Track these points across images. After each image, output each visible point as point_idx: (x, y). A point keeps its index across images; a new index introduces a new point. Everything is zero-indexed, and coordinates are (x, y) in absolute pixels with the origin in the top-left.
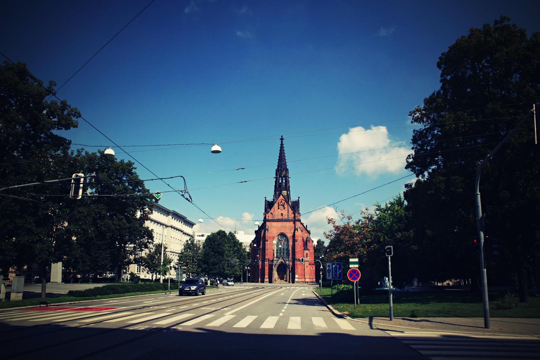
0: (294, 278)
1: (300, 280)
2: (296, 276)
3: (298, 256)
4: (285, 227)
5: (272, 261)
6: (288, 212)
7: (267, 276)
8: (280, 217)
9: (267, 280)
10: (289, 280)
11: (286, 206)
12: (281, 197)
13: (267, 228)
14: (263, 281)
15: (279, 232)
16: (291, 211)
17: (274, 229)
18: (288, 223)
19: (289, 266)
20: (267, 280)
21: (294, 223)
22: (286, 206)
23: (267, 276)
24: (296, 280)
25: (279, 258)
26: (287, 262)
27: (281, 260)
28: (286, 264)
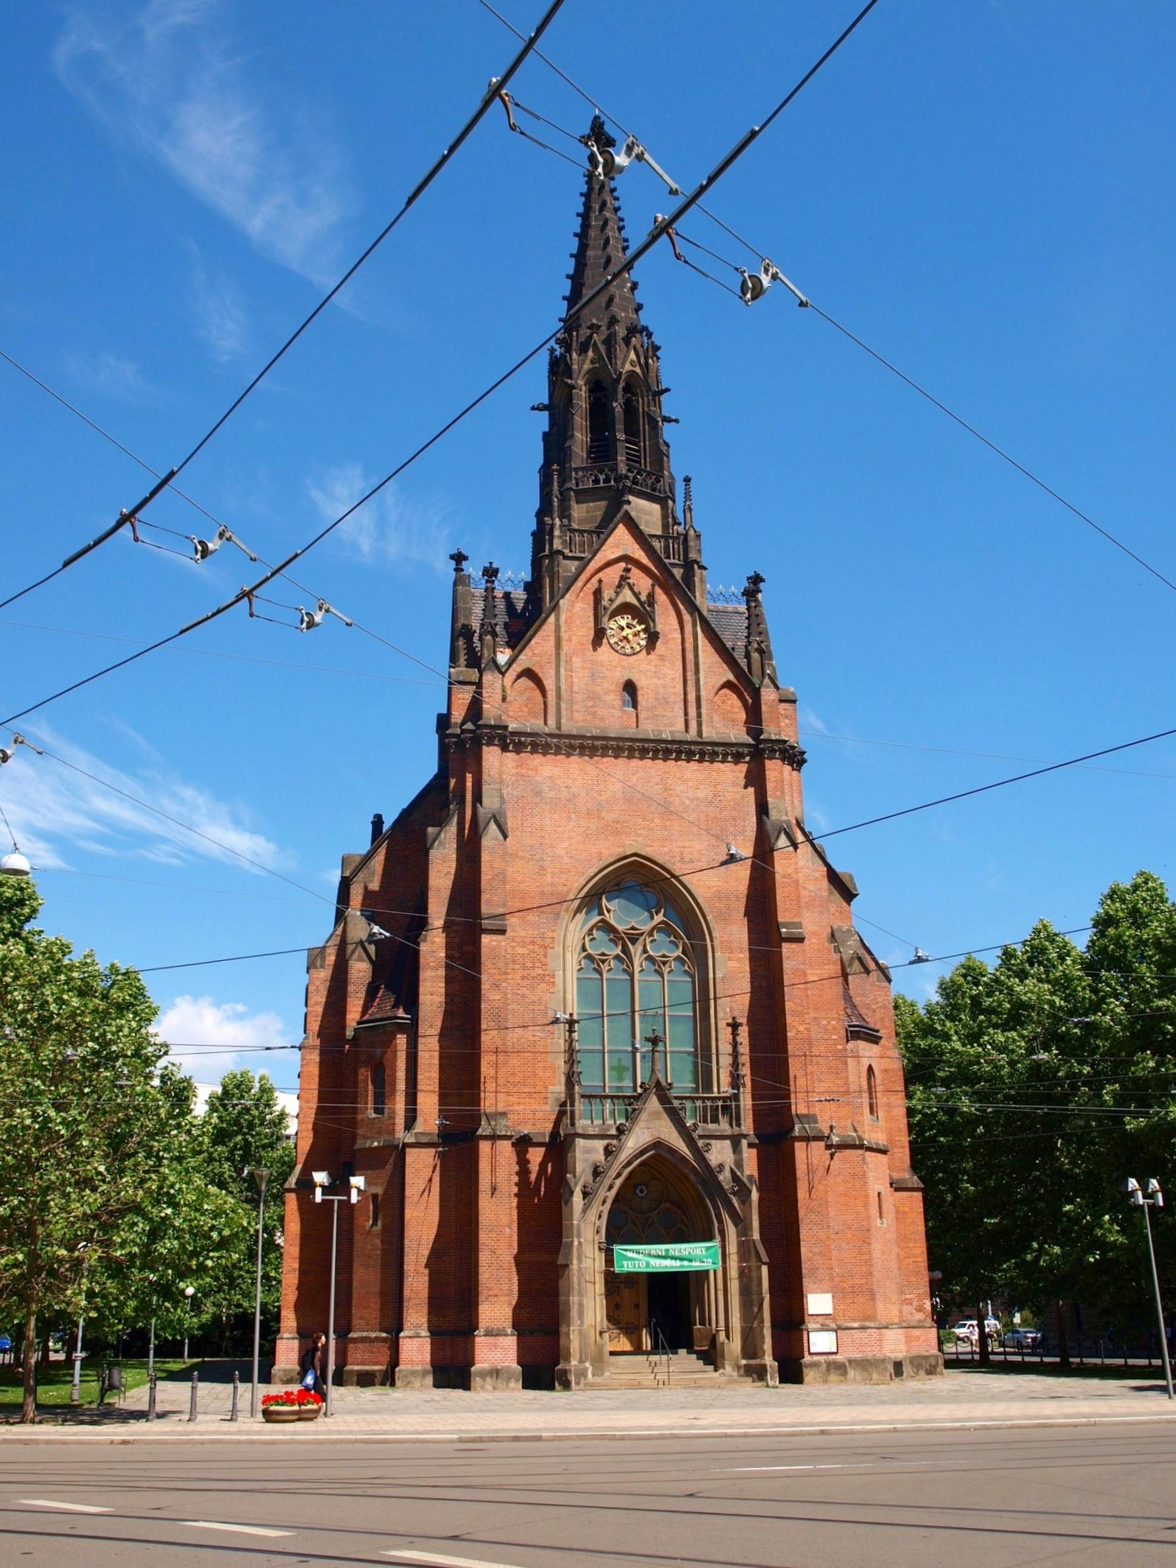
0: (790, 1322)
1: (859, 1345)
2: (818, 1303)
3: (813, 1092)
4: (667, 811)
5: (559, 1146)
6: (690, 669)
7: (496, 1307)
8: (615, 719)
9: (497, 1350)
10: (751, 1349)
11: (666, 619)
12: (621, 541)
13: (490, 802)
14: (453, 1372)
15: (608, 850)
16: (713, 671)
17: (552, 827)
18: (691, 770)
19: (743, 1191)
20: (497, 1350)
21: (756, 779)
22: (666, 619)
23: (496, 1307)
24: (820, 1342)
25: (631, 1104)
26: (720, 1154)
27: (652, 1128)
28: (709, 1174)
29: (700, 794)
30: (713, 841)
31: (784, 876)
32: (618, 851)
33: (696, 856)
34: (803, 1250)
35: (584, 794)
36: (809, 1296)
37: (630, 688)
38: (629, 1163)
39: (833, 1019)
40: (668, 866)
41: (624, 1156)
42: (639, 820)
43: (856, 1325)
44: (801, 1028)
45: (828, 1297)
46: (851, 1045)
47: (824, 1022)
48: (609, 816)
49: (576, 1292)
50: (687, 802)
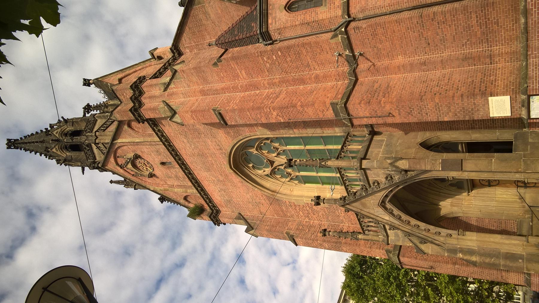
29: (185, 141)
30: (203, 135)
31: (194, 119)
32: (234, 175)
33: (215, 143)
34: (446, 119)
35: (218, 186)
36: (491, 116)
37: (163, 164)
38: (400, 218)
39: (263, 59)
40: (227, 155)
41: (396, 222)
42: (215, 166)
43: (523, 20)
44: (275, 114)
45: (493, 101)
46: (275, 36)
47: (268, 65)
48: (221, 178)
49: (497, 262)
50: (193, 147)
